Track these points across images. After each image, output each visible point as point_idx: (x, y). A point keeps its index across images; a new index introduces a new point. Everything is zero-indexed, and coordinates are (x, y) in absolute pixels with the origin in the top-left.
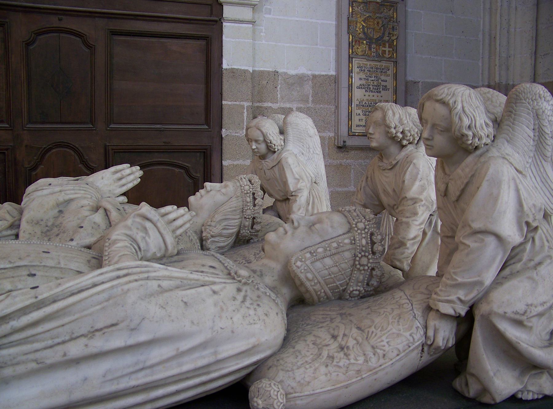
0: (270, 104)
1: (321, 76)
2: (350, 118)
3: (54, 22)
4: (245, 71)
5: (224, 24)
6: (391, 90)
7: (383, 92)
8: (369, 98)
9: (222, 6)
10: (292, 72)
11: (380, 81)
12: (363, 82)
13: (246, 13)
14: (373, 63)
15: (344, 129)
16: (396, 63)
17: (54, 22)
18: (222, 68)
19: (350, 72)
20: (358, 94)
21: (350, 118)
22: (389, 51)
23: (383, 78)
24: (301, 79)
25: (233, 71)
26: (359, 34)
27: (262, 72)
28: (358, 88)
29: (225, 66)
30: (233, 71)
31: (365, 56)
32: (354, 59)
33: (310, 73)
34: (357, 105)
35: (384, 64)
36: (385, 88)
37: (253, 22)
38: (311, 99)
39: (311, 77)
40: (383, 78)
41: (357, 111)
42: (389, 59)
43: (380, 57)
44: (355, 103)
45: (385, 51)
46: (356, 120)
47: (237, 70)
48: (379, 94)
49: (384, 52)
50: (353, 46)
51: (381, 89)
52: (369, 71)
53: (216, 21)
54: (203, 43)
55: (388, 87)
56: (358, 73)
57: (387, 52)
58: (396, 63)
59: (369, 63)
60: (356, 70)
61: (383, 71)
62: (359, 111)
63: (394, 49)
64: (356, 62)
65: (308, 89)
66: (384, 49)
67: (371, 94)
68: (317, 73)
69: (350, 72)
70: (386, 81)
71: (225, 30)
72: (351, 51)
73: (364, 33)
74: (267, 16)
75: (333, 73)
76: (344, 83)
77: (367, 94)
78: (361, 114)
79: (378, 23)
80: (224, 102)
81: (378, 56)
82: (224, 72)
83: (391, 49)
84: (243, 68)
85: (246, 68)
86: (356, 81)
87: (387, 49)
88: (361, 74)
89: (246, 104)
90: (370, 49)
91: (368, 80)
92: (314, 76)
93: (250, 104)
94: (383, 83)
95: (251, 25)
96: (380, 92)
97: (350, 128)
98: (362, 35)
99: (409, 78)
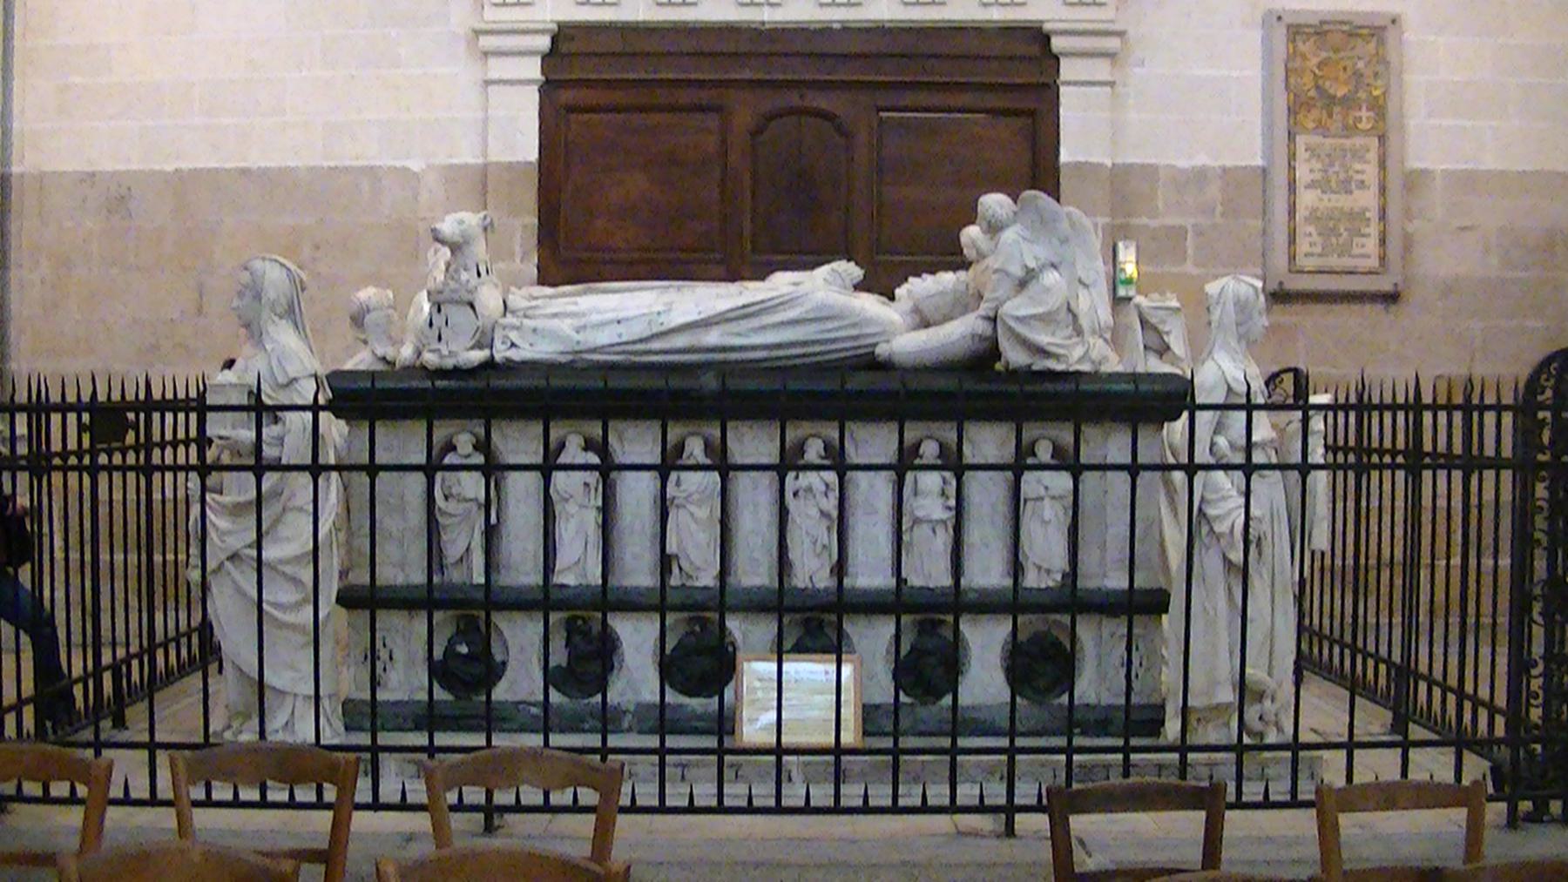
0: (1145, 220)
2: (1292, 240)
5: (1062, 89)
7: (1357, 193)
8: (1330, 205)
9: (1058, 59)
10: (1182, 163)
11: (1351, 173)
12: (1318, 176)
13: (1101, 69)
15: (1280, 261)
16: (1382, 139)
19: (1292, 156)
20: (1307, 199)
21: (1292, 240)
22: (1368, 118)
23: (1358, 166)
24: (1200, 176)
26: (1309, 90)
28: (1308, 187)
29: (1065, 156)
30: (1078, 166)
31: (1321, 129)
32: (1298, 138)
33: (1217, 164)
34: (1306, 219)
35: (1358, 141)
36: (1362, 185)
37: (1112, 84)
38: (1219, 209)
39: (1219, 171)
40: (1358, 166)
41: (1304, 229)
42: (1367, 133)
43: (1350, 130)
44: (1301, 214)
45: (1361, 118)
46: (1303, 246)
48: (1350, 197)
50: (1296, 113)
51: (1353, 186)
52: (1329, 156)
53: (1045, 86)
55: (1366, 183)
56: (1308, 160)
57: (1364, 119)
58: (1382, 139)
60: (1301, 153)
61: (1358, 155)
62: (1311, 229)
63: (1379, 109)
64: (1301, 140)
65: (1214, 191)
66: (1358, 114)
67: (1334, 197)
68: (1229, 163)
71: (1062, 100)
72: (1292, 122)
73: (1318, 87)
74: (1137, 70)
75: (1258, 162)
76: (1280, 177)
77: (1325, 197)
78: (1314, 233)
79: (1345, 69)
81: (1346, 127)
83: (1371, 114)
85: (1100, 161)
86: (1303, 173)
87: (1364, 113)
88: (1314, 161)
91: (1326, 171)
92: (1225, 170)
93: (1107, 220)
94: (1359, 177)
96: (1351, 192)
97: (1292, 258)
98: (1312, 93)
99: (1414, 164)
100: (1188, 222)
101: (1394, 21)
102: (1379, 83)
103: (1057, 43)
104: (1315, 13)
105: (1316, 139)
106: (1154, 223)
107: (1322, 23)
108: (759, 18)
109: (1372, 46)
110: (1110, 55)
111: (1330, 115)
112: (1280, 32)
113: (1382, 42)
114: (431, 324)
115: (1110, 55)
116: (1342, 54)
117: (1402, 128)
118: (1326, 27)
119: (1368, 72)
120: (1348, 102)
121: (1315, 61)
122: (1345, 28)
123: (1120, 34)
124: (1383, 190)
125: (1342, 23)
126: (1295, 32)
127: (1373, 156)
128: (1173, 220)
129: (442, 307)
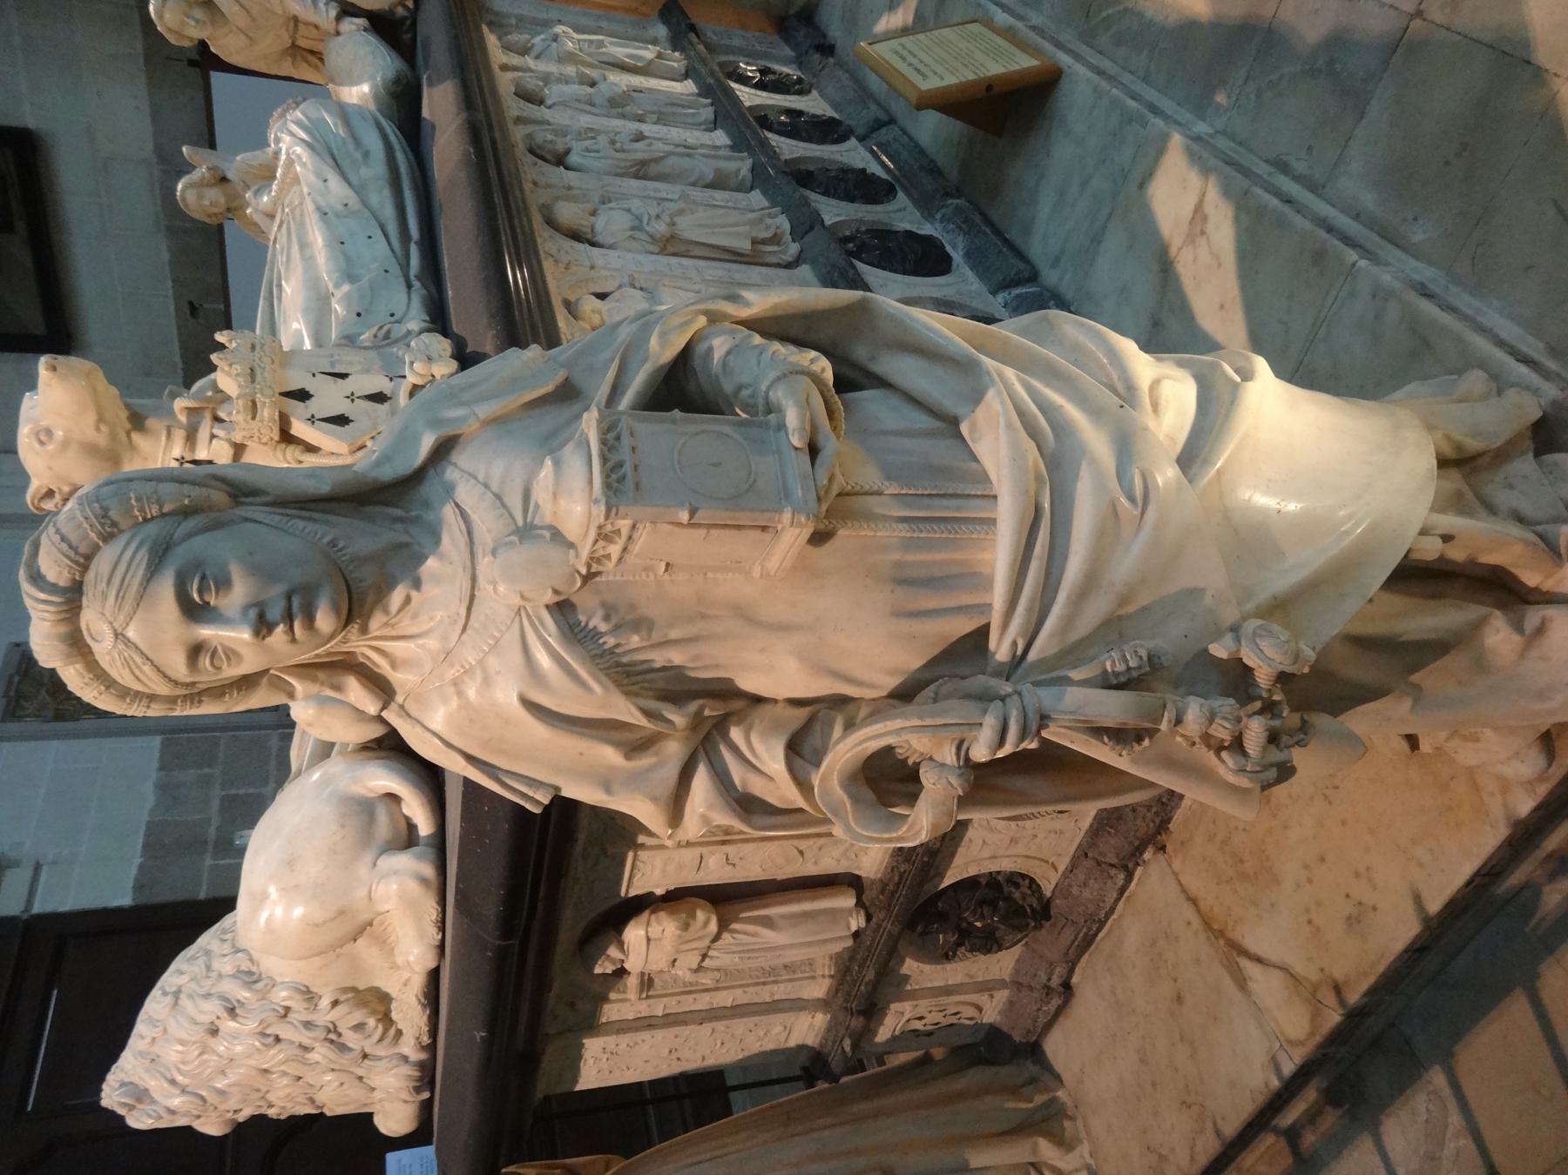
1: (161, 759)
4: (141, 867)
5: (37, 908)
10: (150, 800)
18: (131, 907)
24: (163, 788)
25: (139, 887)
29: (126, 900)
37: (37, 868)
38: (207, 770)
39: (163, 773)
47: (136, 880)
68: (156, 765)
80: (202, 896)
84: (133, 871)
92: (161, 769)
95: (45, 868)
100: (217, 793)
106: (215, 822)
107: (6, 695)
112: (14, 727)
114: (341, 420)
118: (12, 693)
122: (16, 679)
128: (215, 804)
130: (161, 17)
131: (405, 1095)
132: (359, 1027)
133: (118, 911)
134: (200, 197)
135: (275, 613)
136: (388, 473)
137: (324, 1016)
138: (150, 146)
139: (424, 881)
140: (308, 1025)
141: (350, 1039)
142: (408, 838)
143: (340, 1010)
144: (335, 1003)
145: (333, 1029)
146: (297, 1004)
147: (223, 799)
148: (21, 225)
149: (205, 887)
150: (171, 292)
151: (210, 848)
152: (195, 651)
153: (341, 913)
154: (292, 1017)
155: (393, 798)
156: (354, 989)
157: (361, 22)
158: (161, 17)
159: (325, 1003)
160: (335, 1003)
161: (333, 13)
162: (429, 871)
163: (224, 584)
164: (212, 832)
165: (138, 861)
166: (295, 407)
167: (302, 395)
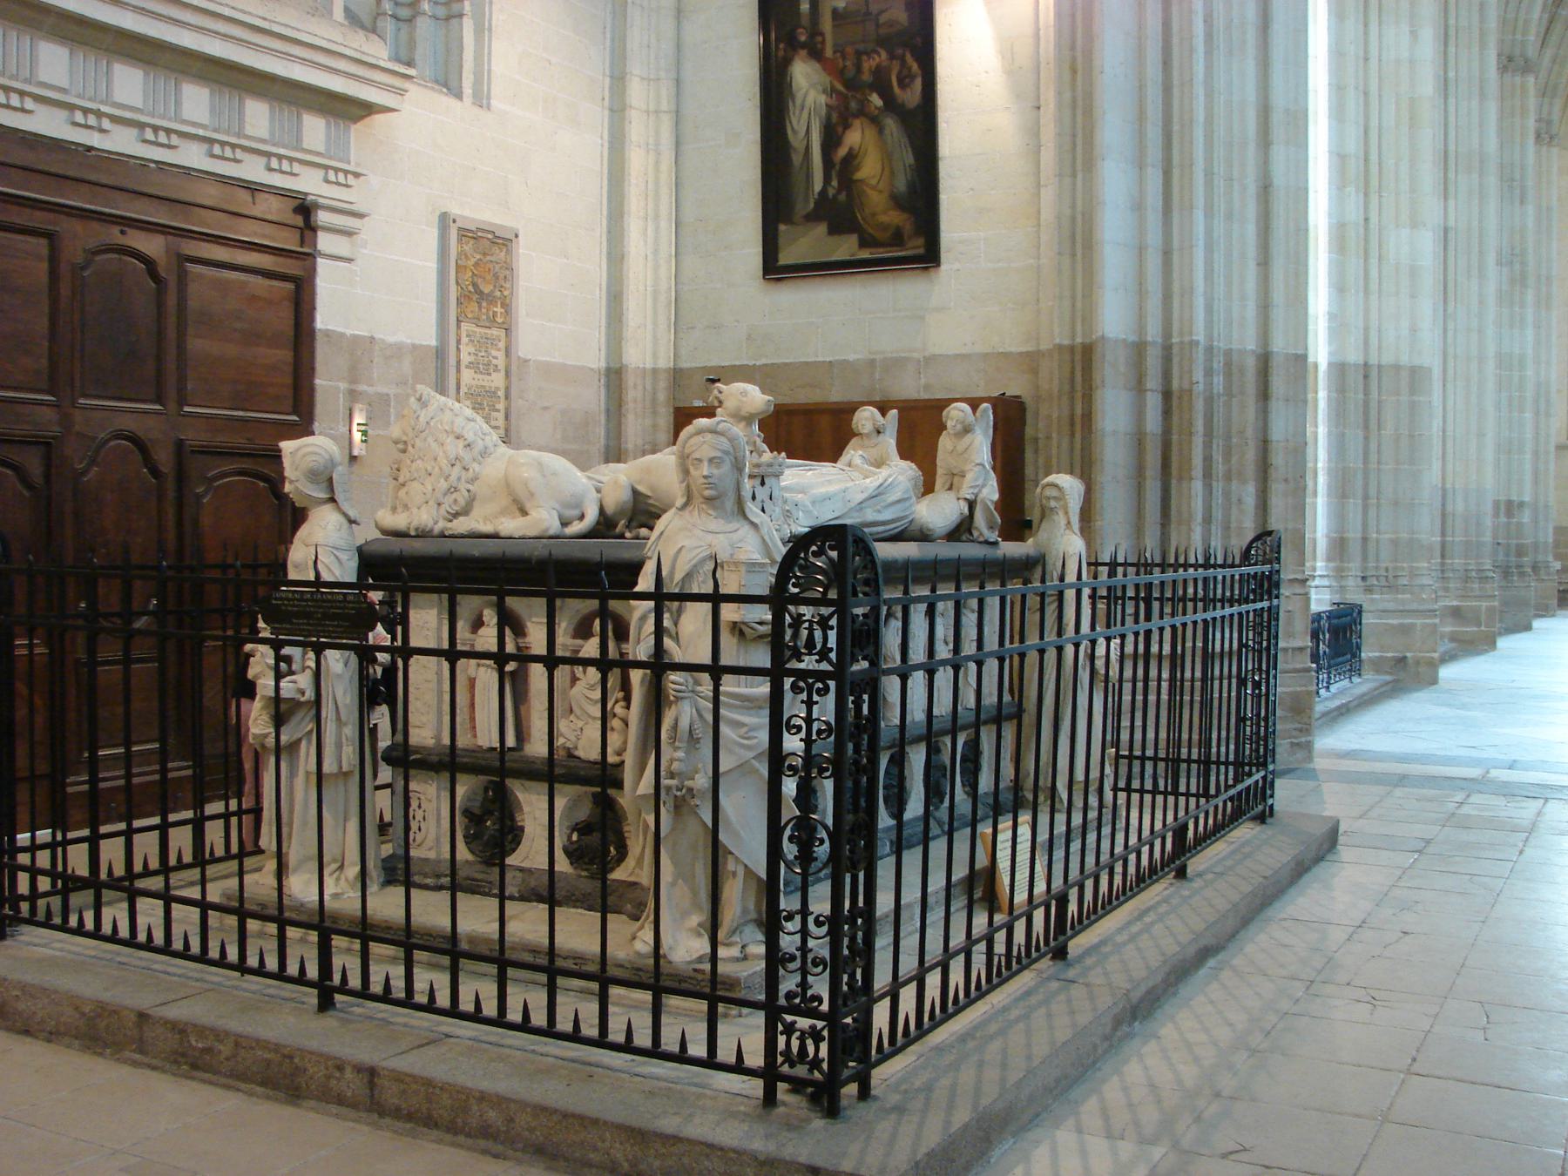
1: (421, 346)
3: (115, 235)
4: (342, 335)
6: (503, 372)
10: (391, 339)
12: (472, 359)
14: (483, 330)
17: (115, 235)
25: (328, 333)
27: (355, 337)
28: (467, 367)
29: (320, 324)
31: (477, 321)
35: (495, 332)
36: (496, 369)
40: (494, 353)
49: (495, 313)
54: (290, 286)
59: (478, 330)
60: (465, 339)
61: (493, 342)
63: (507, 307)
67: (480, 376)
68: (417, 342)
69: (459, 342)
70: (496, 358)
73: (474, 285)
80: (318, 381)
82: (319, 336)
87: (499, 310)
89: (343, 386)
90: (480, 307)
92: (415, 347)
94: (494, 361)
96: (489, 374)
98: (471, 288)
101: (517, 236)
102: (508, 285)
103: (323, 217)
104: (473, 220)
105: (473, 328)
106: (370, 390)
108: (89, 143)
109: (503, 254)
110: (349, 233)
111: (480, 307)
113: (509, 252)
115: (349, 233)
116: (488, 258)
117: (517, 323)
119: (502, 276)
120: (490, 299)
121: (473, 260)
122: (490, 236)
123: (360, 216)
124: (508, 374)
125: (489, 232)
126: (464, 233)
127: (502, 345)
128: (385, 390)
129: (766, 480)
130: (955, 408)
131: (415, 523)
132: (455, 501)
133: (312, 319)
134: (866, 419)
135: (710, 480)
136: (747, 511)
137: (463, 486)
138: (937, 351)
139: (547, 530)
140: (459, 479)
141: (450, 498)
142: (565, 523)
143: (466, 494)
144: (469, 491)
145: (456, 490)
146: (470, 474)
147: (388, 395)
148: (865, 254)
149: (324, 383)
150: (820, 359)
151: (354, 387)
152: (700, 460)
153: (532, 495)
154: (464, 472)
155: (582, 517)
156: (473, 500)
157: (966, 511)
158: (955, 408)
159: (470, 487)
160: (469, 491)
161: (968, 497)
162: (551, 532)
163: (718, 467)
164: (362, 387)
165: (349, 332)
166: (758, 481)
167: (763, 484)
